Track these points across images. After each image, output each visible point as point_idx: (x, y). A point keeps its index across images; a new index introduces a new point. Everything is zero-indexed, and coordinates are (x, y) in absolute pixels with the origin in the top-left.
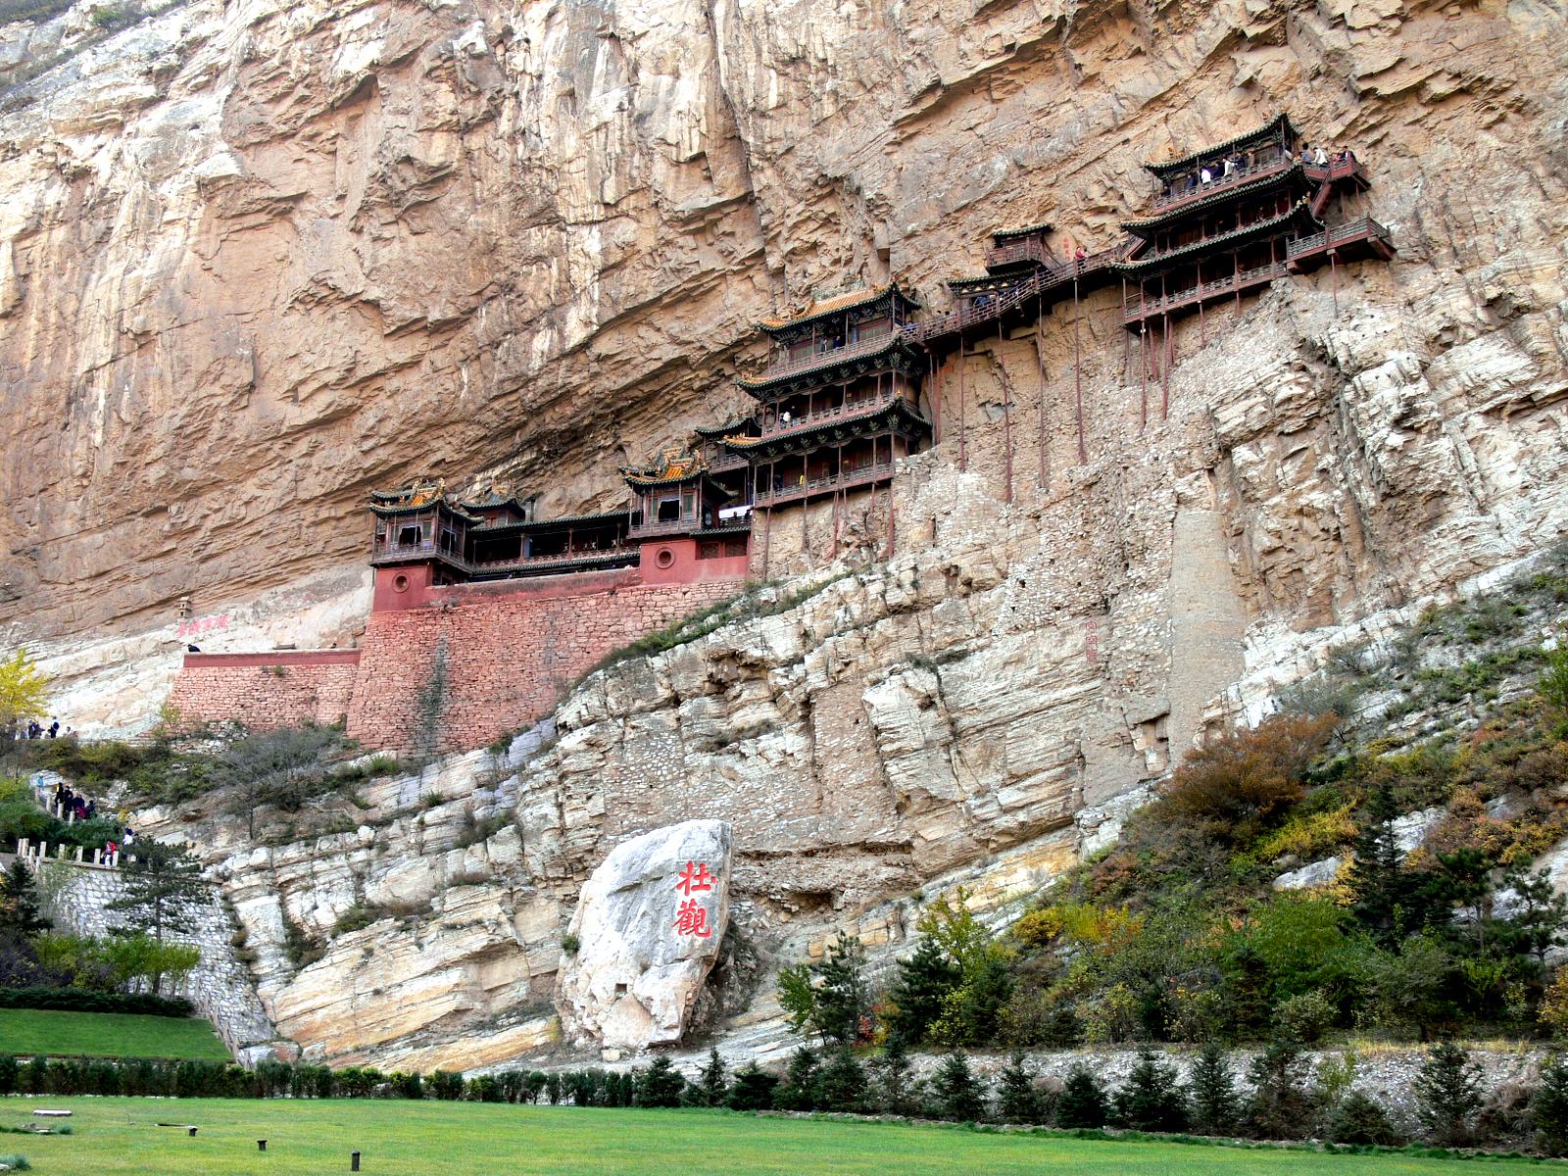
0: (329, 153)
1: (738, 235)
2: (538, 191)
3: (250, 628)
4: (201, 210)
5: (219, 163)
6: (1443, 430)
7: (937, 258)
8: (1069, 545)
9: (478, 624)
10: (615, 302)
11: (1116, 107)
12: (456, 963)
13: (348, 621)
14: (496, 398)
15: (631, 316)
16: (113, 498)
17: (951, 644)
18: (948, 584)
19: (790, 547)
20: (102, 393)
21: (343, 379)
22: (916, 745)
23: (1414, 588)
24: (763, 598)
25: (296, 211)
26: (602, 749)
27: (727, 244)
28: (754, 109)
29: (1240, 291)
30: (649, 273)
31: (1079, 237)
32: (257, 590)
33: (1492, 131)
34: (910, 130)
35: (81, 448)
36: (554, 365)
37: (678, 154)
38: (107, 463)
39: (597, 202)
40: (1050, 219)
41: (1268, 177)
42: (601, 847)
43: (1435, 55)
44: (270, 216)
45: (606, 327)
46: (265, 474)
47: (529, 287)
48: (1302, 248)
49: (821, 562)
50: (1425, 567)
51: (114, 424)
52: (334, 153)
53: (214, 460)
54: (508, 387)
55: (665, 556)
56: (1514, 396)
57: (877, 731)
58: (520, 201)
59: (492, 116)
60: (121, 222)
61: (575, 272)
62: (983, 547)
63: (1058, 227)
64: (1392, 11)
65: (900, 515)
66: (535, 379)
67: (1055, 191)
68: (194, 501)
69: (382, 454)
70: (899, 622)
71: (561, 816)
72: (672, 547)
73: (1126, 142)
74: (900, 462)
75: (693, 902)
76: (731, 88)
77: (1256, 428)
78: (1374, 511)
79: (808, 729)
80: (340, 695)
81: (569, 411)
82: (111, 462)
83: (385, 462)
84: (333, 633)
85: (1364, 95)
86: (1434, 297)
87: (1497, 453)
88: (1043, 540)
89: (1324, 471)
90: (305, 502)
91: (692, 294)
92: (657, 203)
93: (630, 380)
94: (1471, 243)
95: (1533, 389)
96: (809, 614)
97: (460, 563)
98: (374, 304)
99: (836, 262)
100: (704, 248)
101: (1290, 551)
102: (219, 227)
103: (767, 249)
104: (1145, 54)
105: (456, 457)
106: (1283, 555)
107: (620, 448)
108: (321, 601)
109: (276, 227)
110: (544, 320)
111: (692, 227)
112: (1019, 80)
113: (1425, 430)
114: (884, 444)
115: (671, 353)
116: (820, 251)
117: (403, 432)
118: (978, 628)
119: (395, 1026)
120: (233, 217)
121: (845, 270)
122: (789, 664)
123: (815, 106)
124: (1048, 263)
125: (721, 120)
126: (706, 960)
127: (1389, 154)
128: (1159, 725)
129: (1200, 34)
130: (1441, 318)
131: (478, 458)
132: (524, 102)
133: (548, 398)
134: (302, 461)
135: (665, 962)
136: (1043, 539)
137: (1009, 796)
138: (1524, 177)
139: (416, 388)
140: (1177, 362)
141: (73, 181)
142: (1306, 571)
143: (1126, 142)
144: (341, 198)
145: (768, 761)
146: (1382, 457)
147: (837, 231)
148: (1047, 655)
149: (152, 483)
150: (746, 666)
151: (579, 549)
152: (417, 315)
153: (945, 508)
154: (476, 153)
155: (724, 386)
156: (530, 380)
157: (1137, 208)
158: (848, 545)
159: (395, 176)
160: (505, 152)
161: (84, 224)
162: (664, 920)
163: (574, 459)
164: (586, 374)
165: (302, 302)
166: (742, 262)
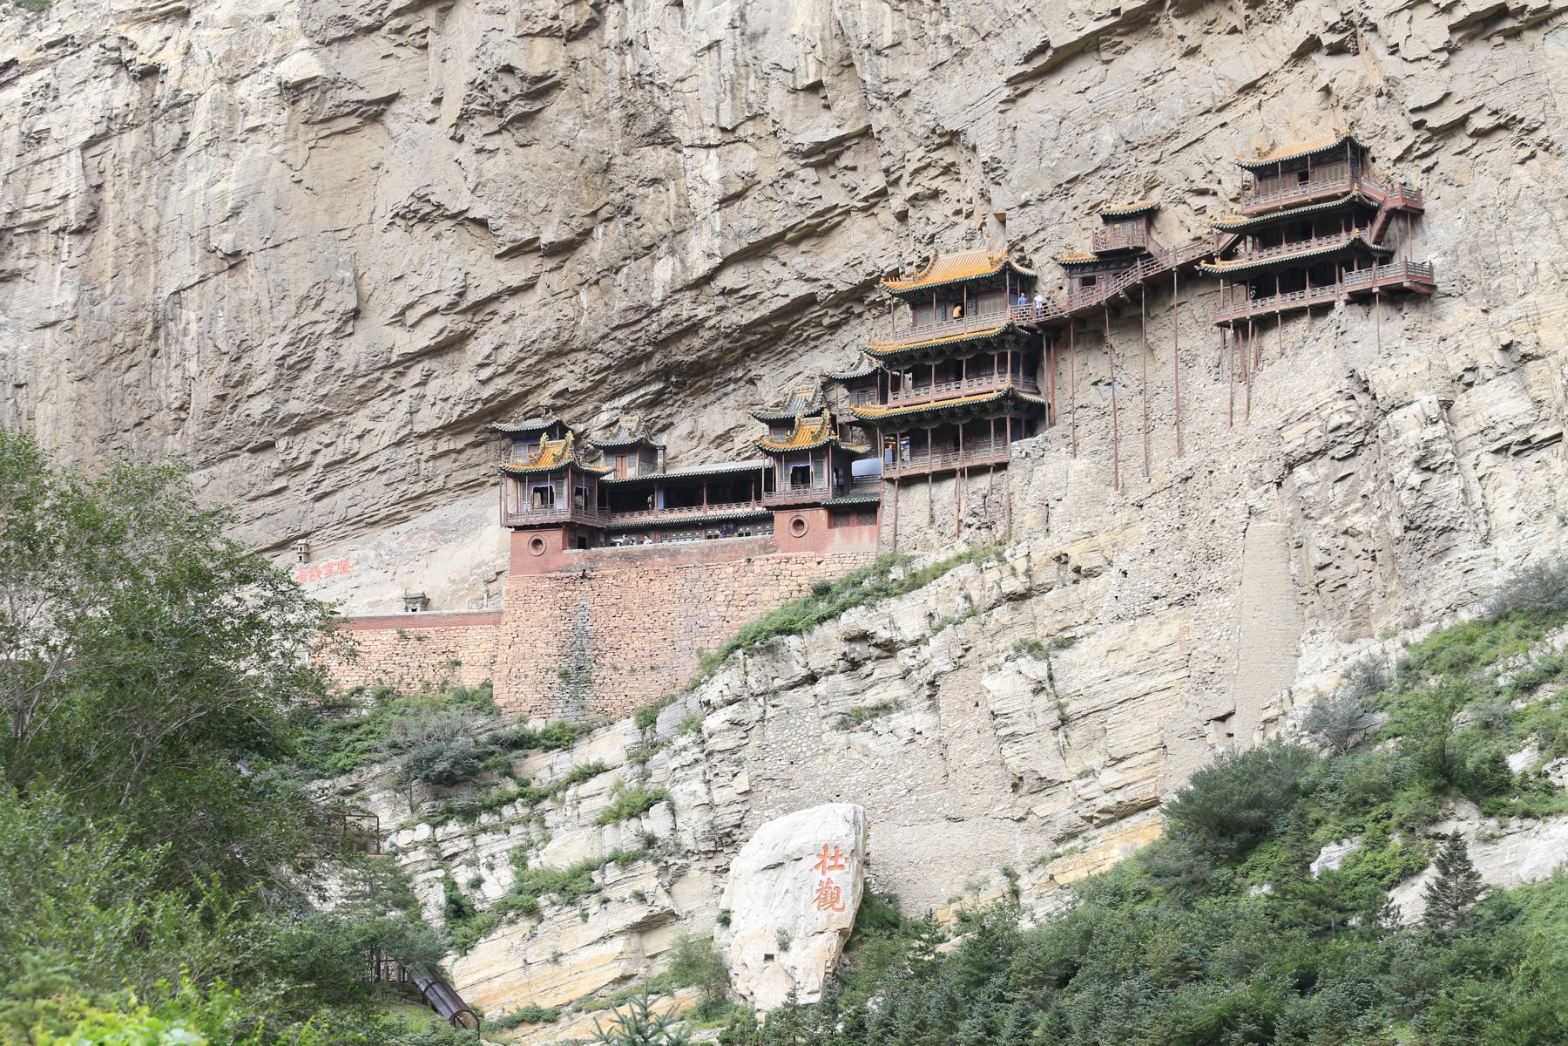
0: (419, 48)
1: (860, 170)
2: (651, 109)
3: (373, 572)
4: (285, 114)
5: (302, 65)
6: (1455, 469)
7: (1050, 230)
8: (1167, 536)
9: (618, 590)
10: (739, 236)
11: (1215, 87)
12: (620, 933)
13: (479, 566)
14: (618, 328)
15: (757, 251)
16: (216, 433)
17: (1061, 630)
18: (1059, 569)
19: (917, 521)
20: (193, 316)
21: (453, 305)
22: (1027, 729)
23: (1426, 613)
24: (891, 577)
25: (388, 113)
26: (745, 728)
27: (850, 178)
28: (869, 46)
29: (1312, 307)
30: (771, 205)
31: (1183, 217)
32: (377, 530)
33: (1525, 166)
34: (1024, 87)
35: (176, 377)
36: (677, 296)
37: (795, 79)
38: (203, 396)
39: (713, 126)
40: (1155, 198)
41: (1335, 197)
42: (747, 822)
43: (1478, 89)
44: (360, 120)
45: (728, 262)
46: (379, 406)
47: (643, 209)
48: (1358, 280)
49: (946, 540)
50: (1435, 594)
51: (209, 352)
52: (425, 47)
53: (322, 391)
54: (632, 317)
55: (798, 524)
56: (1520, 437)
57: (994, 715)
58: (632, 117)
59: (593, 24)
60: (199, 125)
61: (695, 199)
62: (1090, 534)
63: (1163, 206)
64: (1440, 45)
65: (1016, 499)
66: (658, 310)
67: (1159, 167)
68: (303, 435)
69: (501, 383)
70: (1013, 609)
71: (709, 792)
72: (805, 515)
73: (1223, 125)
74: (1018, 447)
75: (829, 880)
76: (845, 19)
77: (1313, 451)
78: (1399, 541)
79: (934, 708)
80: (484, 659)
81: (697, 343)
82: (211, 395)
83: (505, 392)
84: (464, 580)
85: (1418, 126)
86: (1462, 336)
87: (1500, 490)
88: (1144, 528)
89: (1364, 496)
90: (422, 436)
91: (816, 230)
92: (775, 133)
93: (756, 316)
94: (1496, 282)
95: (1531, 433)
96: (928, 595)
97: (597, 521)
98: (482, 223)
99: (958, 212)
100: (825, 178)
101: (1338, 567)
102: (307, 133)
103: (890, 190)
104: (1241, 32)
105: (580, 386)
106: (1331, 571)
107: (752, 382)
108: (446, 542)
109: (368, 131)
110: (664, 246)
111: (812, 160)
112: (1127, 41)
113: (1440, 470)
114: (1000, 429)
115: (799, 290)
116: (942, 198)
117: (522, 360)
118: (1086, 615)
119: (567, 991)
120: (322, 122)
121: (966, 222)
122: (915, 643)
123: (931, 48)
124: (1151, 249)
125: (837, 46)
126: (842, 932)
127: (1439, 181)
128: (1227, 722)
129: (1285, 28)
130: (1464, 358)
131: (599, 387)
132: (630, 8)
133: (673, 330)
134: (416, 391)
135: (807, 935)
136: (1144, 528)
137: (1110, 777)
138: (1545, 218)
139: (533, 314)
140: (1260, 366)
141: (140, 79)
142: (1349, 587)
143: (1223, 125)
144: (437, 101)
145: (900, 738)
146: (1405, 494)
147: (958, 180)
148: (1145, 644)
149: (257, 417)
150: (877, 645)
151: (715, 500)
152: (528, 235)
153: (1058, 495)
154: (582, 64)
155: (854, 322)
156: (653, 311)
157: (1233, 196)
158: (969, 526)
159: (495, 84)
160: (613, 62)
161: (158, 128)
162: (804, 897)
163: (705, 390)
164: (711, 306)
165: (403, 217)
166: (866, 199)
